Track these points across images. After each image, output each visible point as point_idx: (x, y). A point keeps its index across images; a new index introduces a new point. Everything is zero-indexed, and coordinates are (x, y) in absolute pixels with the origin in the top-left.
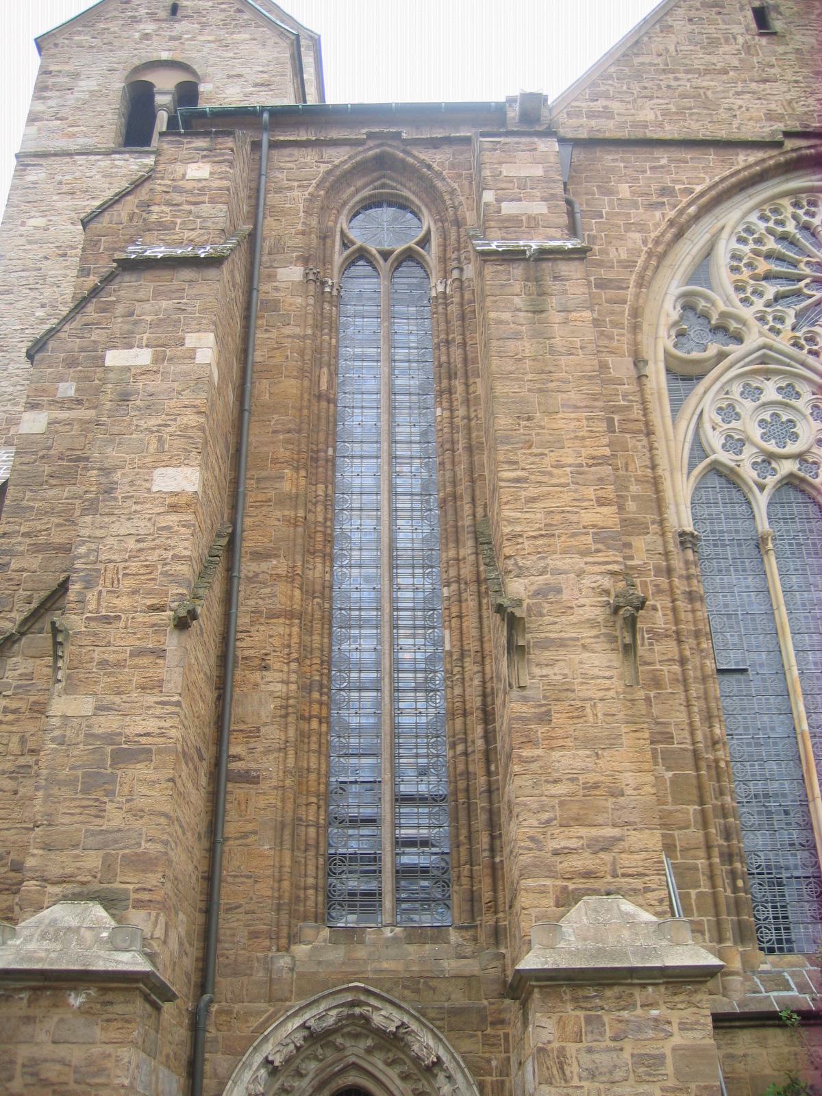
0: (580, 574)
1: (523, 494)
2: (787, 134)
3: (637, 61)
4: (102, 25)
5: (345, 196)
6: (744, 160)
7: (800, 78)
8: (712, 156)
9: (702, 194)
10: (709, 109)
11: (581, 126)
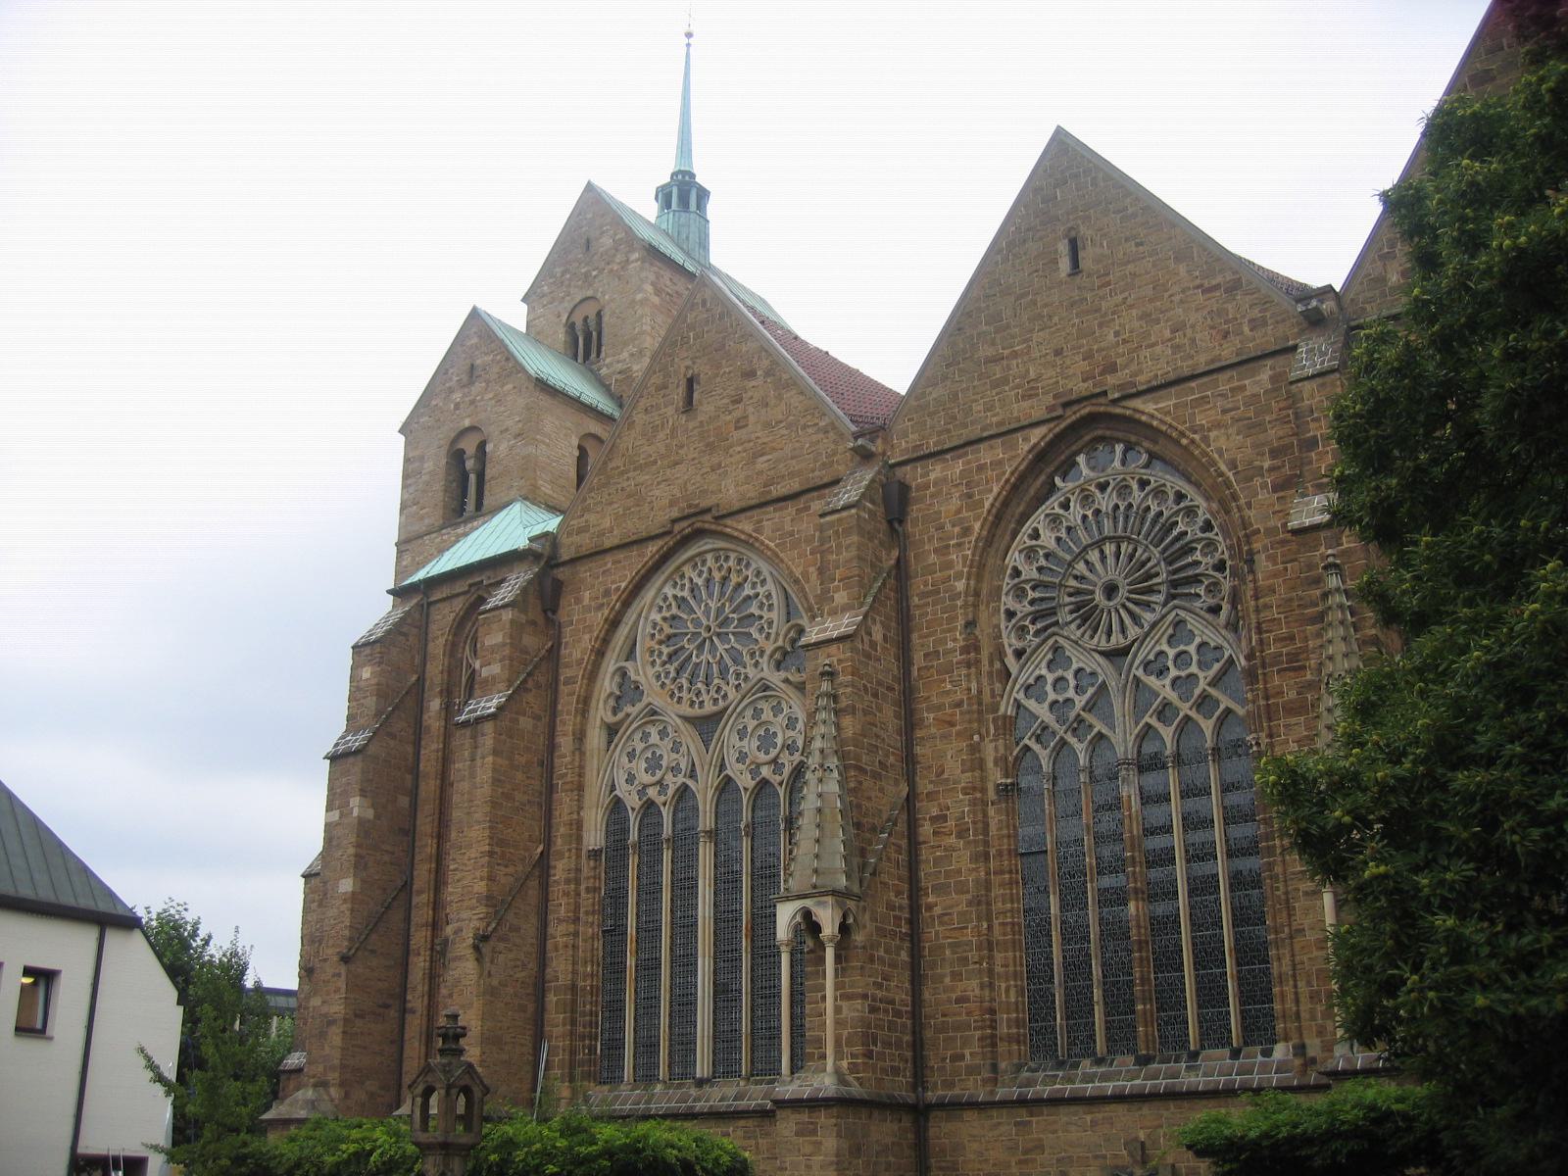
2: (674, 521)
3: (611, 465)
6: (652, 549)
9: (625, 589)
10: (638, 505)
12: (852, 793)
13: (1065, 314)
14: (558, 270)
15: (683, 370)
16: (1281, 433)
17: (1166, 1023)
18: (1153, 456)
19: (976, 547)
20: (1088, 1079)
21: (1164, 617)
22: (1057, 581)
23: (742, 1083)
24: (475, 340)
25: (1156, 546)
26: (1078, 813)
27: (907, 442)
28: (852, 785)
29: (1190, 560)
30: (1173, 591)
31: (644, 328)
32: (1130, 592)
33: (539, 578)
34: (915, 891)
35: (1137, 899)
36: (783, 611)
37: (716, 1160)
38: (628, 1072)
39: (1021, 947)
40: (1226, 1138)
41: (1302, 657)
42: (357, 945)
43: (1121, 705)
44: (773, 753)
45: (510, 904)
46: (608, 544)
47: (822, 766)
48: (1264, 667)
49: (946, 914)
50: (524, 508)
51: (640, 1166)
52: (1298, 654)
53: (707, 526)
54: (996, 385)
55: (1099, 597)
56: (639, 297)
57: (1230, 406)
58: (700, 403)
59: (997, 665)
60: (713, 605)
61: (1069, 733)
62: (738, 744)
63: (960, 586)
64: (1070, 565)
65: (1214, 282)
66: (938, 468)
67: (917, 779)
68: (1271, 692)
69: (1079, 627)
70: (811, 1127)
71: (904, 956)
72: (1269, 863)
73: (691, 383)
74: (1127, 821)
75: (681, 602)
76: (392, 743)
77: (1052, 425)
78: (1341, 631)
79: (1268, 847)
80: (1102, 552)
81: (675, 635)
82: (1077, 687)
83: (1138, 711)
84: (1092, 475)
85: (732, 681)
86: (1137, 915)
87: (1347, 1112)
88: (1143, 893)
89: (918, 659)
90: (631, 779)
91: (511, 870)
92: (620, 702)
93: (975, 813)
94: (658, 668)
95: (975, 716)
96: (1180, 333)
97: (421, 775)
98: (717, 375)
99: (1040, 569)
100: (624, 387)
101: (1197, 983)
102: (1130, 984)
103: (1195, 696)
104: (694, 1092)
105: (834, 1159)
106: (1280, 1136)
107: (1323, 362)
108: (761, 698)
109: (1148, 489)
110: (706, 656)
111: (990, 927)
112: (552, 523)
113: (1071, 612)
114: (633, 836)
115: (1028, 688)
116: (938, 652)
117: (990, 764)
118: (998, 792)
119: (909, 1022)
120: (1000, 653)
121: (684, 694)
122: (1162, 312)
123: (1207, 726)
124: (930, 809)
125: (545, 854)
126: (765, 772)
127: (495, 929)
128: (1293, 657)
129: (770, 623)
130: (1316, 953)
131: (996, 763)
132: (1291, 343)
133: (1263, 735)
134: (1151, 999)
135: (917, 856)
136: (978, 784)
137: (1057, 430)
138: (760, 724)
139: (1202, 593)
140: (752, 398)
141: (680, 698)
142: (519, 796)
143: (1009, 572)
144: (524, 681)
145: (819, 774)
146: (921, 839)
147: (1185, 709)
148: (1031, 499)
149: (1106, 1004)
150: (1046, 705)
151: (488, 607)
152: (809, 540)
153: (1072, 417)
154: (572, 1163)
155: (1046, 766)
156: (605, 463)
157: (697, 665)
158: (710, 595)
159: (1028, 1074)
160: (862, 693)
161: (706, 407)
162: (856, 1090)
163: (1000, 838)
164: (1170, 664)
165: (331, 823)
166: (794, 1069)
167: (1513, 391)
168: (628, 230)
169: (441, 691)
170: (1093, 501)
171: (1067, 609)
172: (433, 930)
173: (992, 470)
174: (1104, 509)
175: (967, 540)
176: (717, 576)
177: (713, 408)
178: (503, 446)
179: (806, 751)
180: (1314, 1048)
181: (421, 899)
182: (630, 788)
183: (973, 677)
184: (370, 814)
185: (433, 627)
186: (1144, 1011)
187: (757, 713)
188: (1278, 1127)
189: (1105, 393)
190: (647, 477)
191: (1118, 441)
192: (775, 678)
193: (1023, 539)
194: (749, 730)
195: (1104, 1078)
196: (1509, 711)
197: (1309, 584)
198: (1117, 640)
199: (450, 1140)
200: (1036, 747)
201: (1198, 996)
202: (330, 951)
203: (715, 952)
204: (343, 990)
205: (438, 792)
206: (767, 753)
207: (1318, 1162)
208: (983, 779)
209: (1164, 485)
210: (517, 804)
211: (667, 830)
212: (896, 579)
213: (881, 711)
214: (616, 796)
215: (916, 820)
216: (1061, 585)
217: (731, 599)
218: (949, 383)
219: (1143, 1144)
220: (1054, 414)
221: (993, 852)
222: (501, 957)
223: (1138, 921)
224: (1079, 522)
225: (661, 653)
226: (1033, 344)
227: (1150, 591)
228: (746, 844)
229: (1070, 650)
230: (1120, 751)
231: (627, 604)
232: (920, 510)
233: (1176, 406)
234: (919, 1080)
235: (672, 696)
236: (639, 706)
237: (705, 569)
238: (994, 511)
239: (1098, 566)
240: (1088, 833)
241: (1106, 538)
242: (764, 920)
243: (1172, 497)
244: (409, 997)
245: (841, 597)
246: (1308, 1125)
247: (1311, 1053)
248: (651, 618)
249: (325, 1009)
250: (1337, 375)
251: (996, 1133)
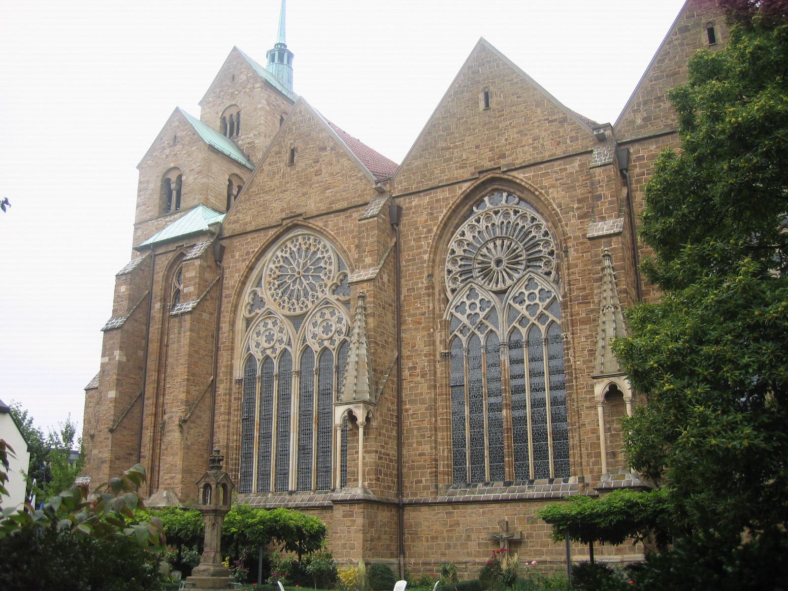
0: (177, 412)
1: (170, 391)
2: (283, 219)
3: (252, 190)
4: (155, 154)
5: (174, 270)
6: (272, 233)
7: (295, 187)
8: (262, 234)
9: (257, 252)
11: (230, 228)
12: (373, 356)
13: (481, 128)
14: (218, 90)
15: (289, 145)
16: (583, 192)
17: (519, 467)
18: (521, 199)
19: (434, 238)
20: (481, 492)
21: (524, 276)
22: (473, 257)
23: (312, 493)
24: (177, 123)
25: (521, 243)
26: (480, 367)
27: (402, 186)
28: (372, 351)
29: (537, 249)
30: (528, 264)
31: (262, 122)
32: (508, 263)
33: (213, 244)
34: (400, 402)
35: (506, 409)
36: (337, 266)
37: (312, 526)
38: (254, 487)
39: (450, 430)
40: (562, 515)
41: (589, 297)
42: (117, 424)
43: (501, 317)
44: (330, 334)
45: (197, 405)
46: (249, 229)
47: (358, 341)
48: (571, 301)
49: (414, 414)
50: (204, 210)
51: (278, 528)
52: (586, 296)
53: (300, 222)
54: (446, 161)
55: (493, 265)
56: (259, 106)
57: (559, 177)
58: (298, 162)
59: (442, 296)
60: (301, 261)
61: (476, 329)
62: (313, 330)
63: (426, 257)
64: (479, 249)
65: (554, 118)
66: (417, 199)
67: (402, 349)
68: (574, 313)
69: (483, 279)
70: (351, 513)
71: (394, 433)
72: (570, 393)
73: (293, 151)
74: (503, 372)
75: (285, 259)
76: (136, 324)
77: (473, 182)
78: (610, 286)
79: (570, 386)
80: (495, 244)
81: (282, 275)
82: (480, 308)
83: (510, 320)
84: (491, 207)
85: (310, 299)
86: (507, 416)
87: (617, 503)
88: (510, 406)
89: (404, 291)
90: (258, 345)
91: (197, 388)
92: (253, 307)
93: (430, 366)
94: (272, 291)
95: (432, 320)
96: (537, 141)
97: (150, 340)
98: (306, 149)
99: (464, 251)
100: (250, 151)
101: (534, 448)
102: (502, 448)
103: (538, 314)
104: (287, 497)
105: (362, 528)
106: (586, 513)
107: (605, 159)
108: (323, 308)
109: (518, 215)
110: (297, 286)
111: (436, 421)
112: (220, 218)
113: (479, 272)
114: (259, 373)
115: (457, 307)
116: (414, 288)
117: (438, 343)
118: (441, 356)
119: (396, 465)
120: (444, 291)
121: (286, 304)
122: (528, 131)
123: (543, 328)
124: (407, 364)
125: (214, 381)
126: (326, 343)
127: (190, 417)
128: (585, 297)
129: (330, 271)
130: (590, 435)
131: (441, 343)
132: (589, 149)
133: (569, 333)
134: (512, 456)
135: (401, 386)
136: (432, 352)
137: (475, 184)
138: (323, 321)
139: (542, 266)
140: (324, 161)
141: (283, 306)
142: (202, 352)
143: (449, 251)
144: (205, 296)
145: (357, 345)
146: (403, 378)
147: (532, 320)
148: (461, 217)
149: (490, 457)
150: (466, 316)
151: (188, 258)
152: (352, 231)
153: (483, 177)
154: (244, 527)
155: (465, 345)
156: (248, 189)
157: (292, 290)
158: (300, 257)
159: (453, 490)
160: (378, 307)
161: (301, 164)
162: (372, 496)
163: (442, 378)
164: (526, 298)
165: (104, 363)
166: (344, 483)
167: (732, 183)
168: (255, 72)
169: (161, 299)
170: (492, 219)
171: (477, 270)
172: (155, 417)
173: (443, 202)
174: (496, 224)
175: (430, 235)
176: (304, 247)
177: (304, 165)
178: (191, 178)
179: (349, 332)
180: (588, 479)
181: (149, 402)
182: (257, 349)
183: (431, 301)
184: (124, 359)
185: (157, 268)
186: (509, 461)
187: (323, 315)
188: (585, 509)
189: (499, 168)
190: (270, 197)
191: (505, 191)
192: (333, 298)
193: (457, 235)
194: (318, 323)
195: (489, 492)
196: (724, 321)
197: (596, 264)
198: (501, 286)
199: (218, 508)
200: (460, 336)
201: (534, 454)
202: (103, 427)
203: (299, 430)
204: (110, 446)
205: (158, 349)
206: (327, 334)
207: (603, 525)
208: (434, 350)
209: (526, 213)
210: (201, 356)
211: (276, 371)
212: (394, 253)
213: (386, 316)
214: (250, 353)
215: (401, 369)
216: (475, 259)
217: (311, 259)
218: (423, 159)
219: (507, 522)
220: (474, 177)
221: (438, 385)
222: (192, 431)
223: (507, 419)
224: (484, 229)
225: (274, 284)
226: (465, 142)
227: (517, 263)
228: (316, 378)
229: (478, 290)
230: (501, 339)
231: (258, 259)
232: (407, 219)
233: (533, 176)
234: (400, 491)
235: (280, 305)
236: (263, 310)
237: (298, 244)
238: (444, 222)
239: (493, 250)
240: (484, 376)
241: (497, 237)
242: (326, 415)
243: (529, 219)
244: (142, 450)
245: (368, 260)
246: (599, 509)
247: (586, 481)
248: (269, 267)
249: (100, 455)
250: (612, 166)
251: (436, 517)
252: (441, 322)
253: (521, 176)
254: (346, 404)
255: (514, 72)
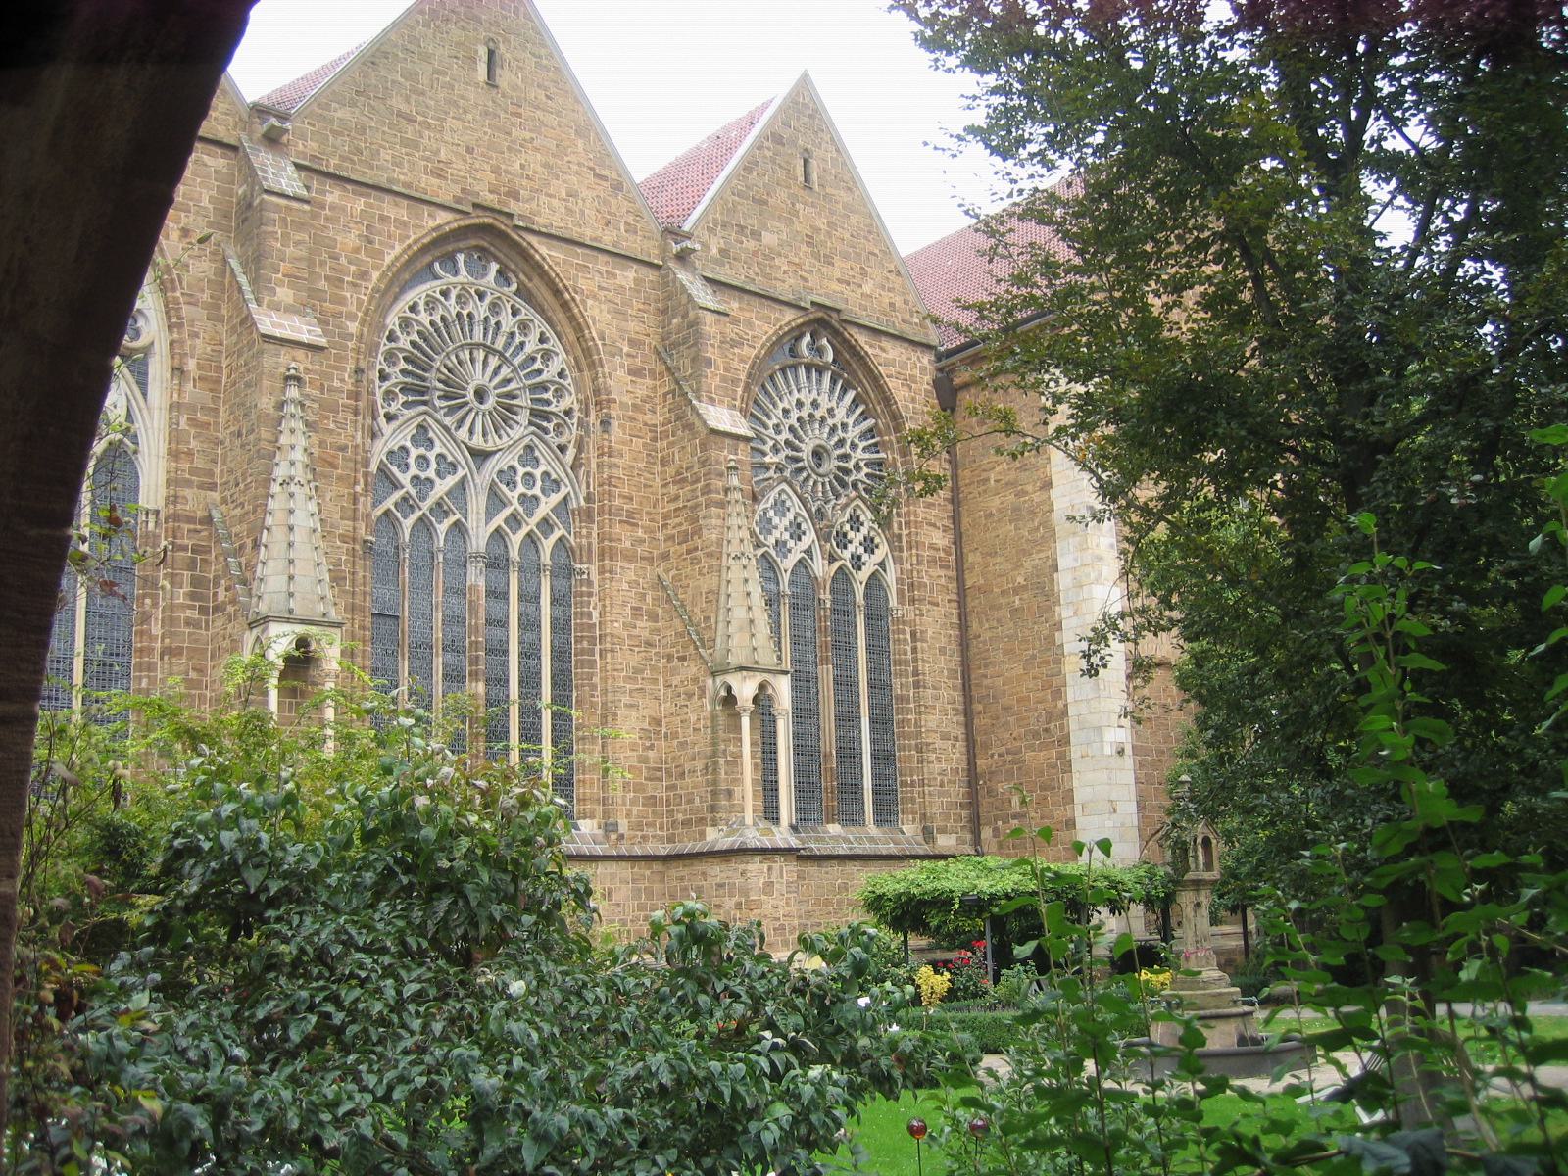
54: (405, 143)
55: (470, 396)
66: (337, 193)
77: (458, 216)
128: (631, 514)
130: (629, 753)
137: (461, 223)
164: (519, 479)
171: (438, 393)
189: (510, 216)
191: (497, 259)
218: (357, 111)
252: (366, 475)
253: (544, 250)
254: (303, 622)
255: (544, 46)
